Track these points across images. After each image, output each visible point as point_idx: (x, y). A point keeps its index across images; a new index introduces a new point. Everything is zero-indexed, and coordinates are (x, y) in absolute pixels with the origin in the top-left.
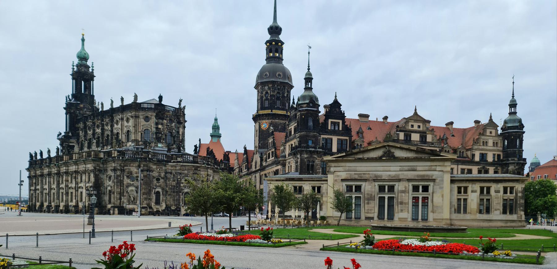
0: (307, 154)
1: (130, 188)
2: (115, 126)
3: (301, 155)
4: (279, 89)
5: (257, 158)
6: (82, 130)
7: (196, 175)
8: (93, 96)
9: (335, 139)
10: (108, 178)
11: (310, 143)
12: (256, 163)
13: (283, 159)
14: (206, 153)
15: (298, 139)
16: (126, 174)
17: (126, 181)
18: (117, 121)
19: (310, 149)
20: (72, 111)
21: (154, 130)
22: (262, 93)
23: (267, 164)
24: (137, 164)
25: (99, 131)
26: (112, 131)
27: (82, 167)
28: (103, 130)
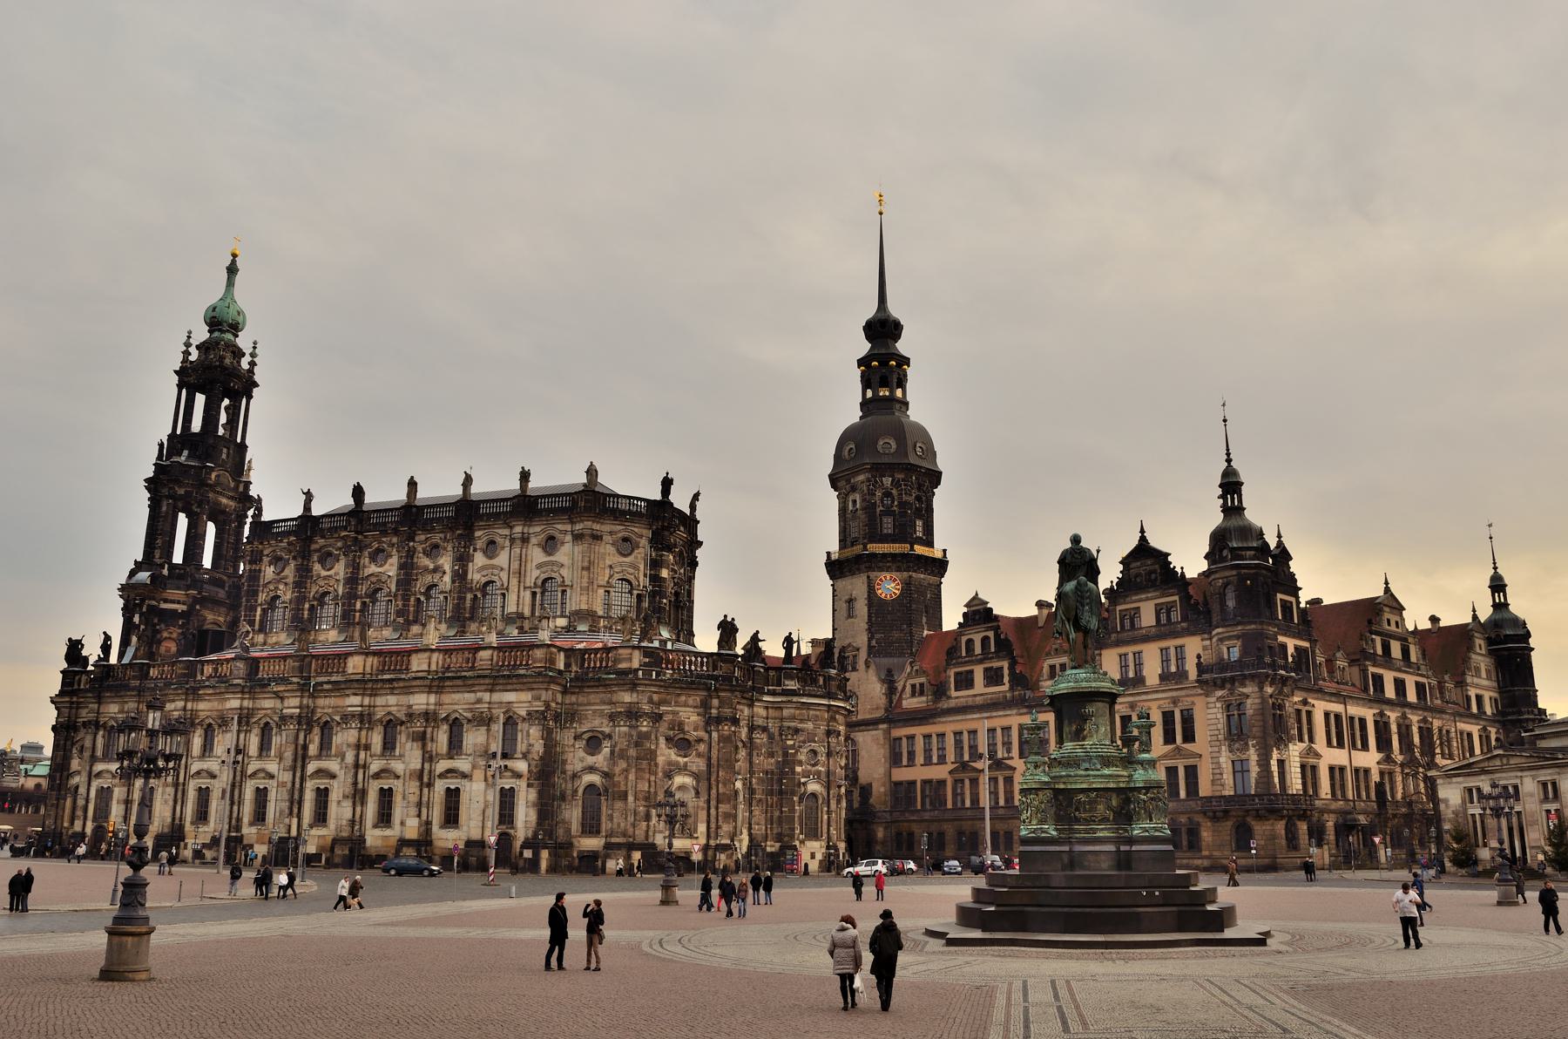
1: (679, 780)
2: (479, 559)
3: (1261, 689)
4: (919, 488)
6: (276, 560)
7: (833, 740)
8: (243, 448)
9: (1291, 644)
10: (581, 744)
16: (663, 727)
17: (666, 754)
18: (492, 542)
20: (181, 492)
21: (644, 581)
23: (944, 705)
24: (695, 698)
25: (391, 568)
26: (460, 576)
27: (458, 702)
28: (407, 567)
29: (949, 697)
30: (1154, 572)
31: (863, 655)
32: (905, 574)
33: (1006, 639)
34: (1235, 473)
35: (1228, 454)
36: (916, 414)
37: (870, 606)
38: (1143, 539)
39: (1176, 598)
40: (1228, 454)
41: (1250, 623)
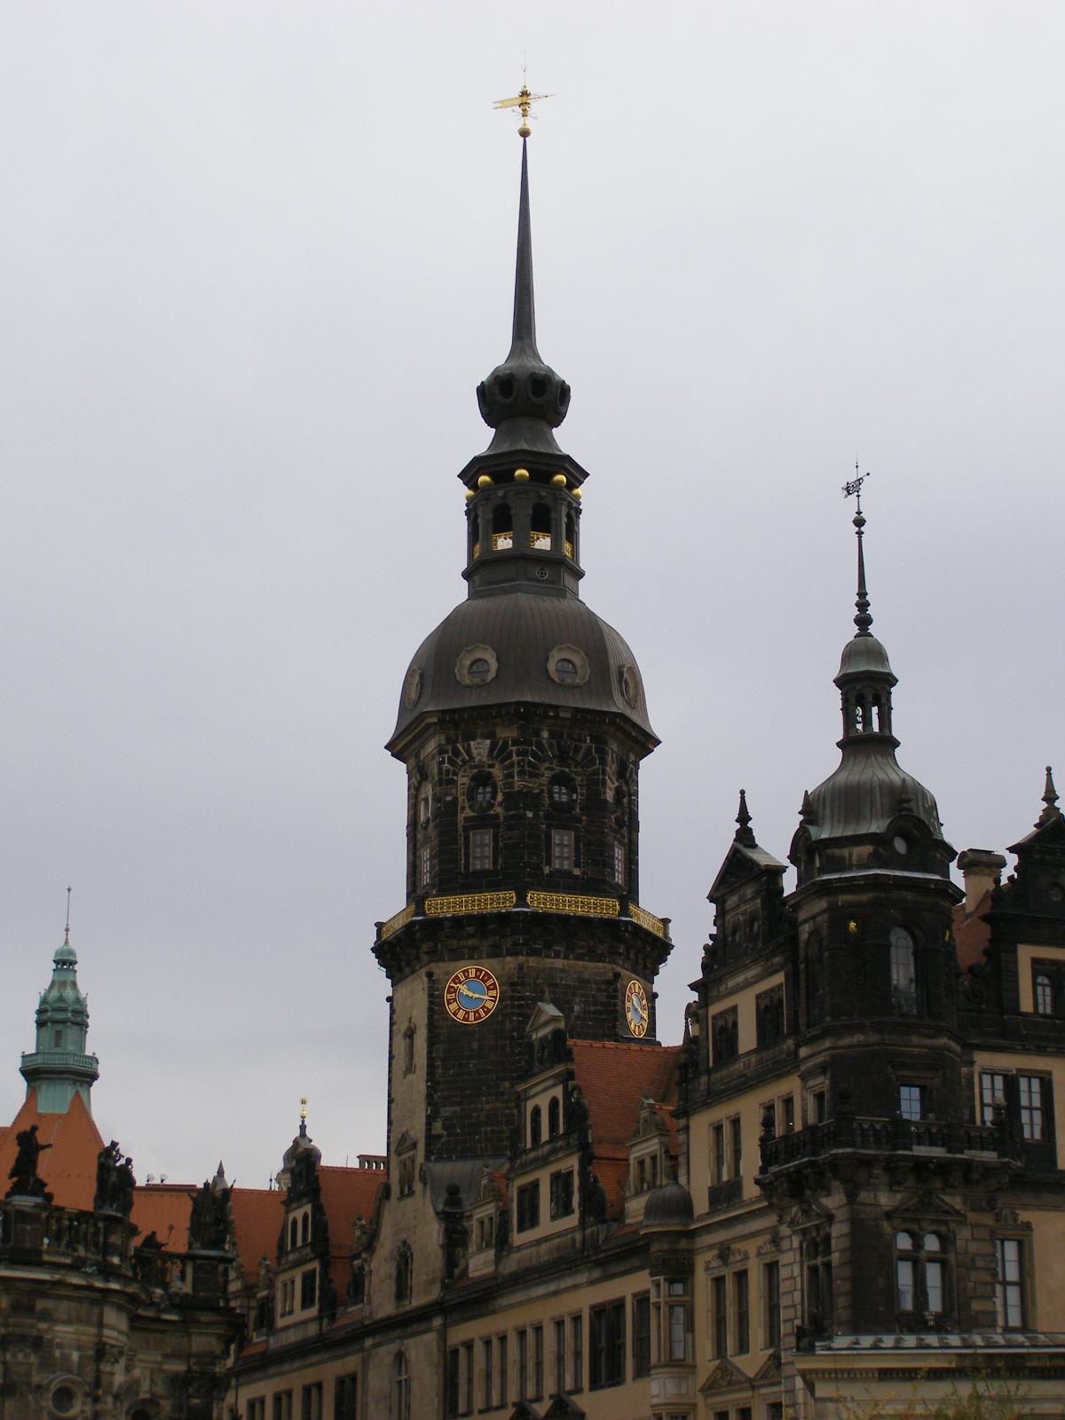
0: (894, 1185)
3: (851, 1197)
4: (563, 758)
5: (417, 1223)
11: (910, 1104)
12: (404, 1259)
13: (674, 1225)
14: (91, 1188)
15: (822, 1082)
19: (922, 1151)
22: (446, 781)
23: (511, 1264)
29: (511, 1249)
30: (753, 919)
31: (420, 1158)
32: (511, 962)
33: (578, 1102)
34: (879, 654)
35: (863, 605)
36: (599, 591)
37: (432, 1042)
38: (745, 836)
39: (779, 978)
40: (863, 605)
41: (849, 1029)
